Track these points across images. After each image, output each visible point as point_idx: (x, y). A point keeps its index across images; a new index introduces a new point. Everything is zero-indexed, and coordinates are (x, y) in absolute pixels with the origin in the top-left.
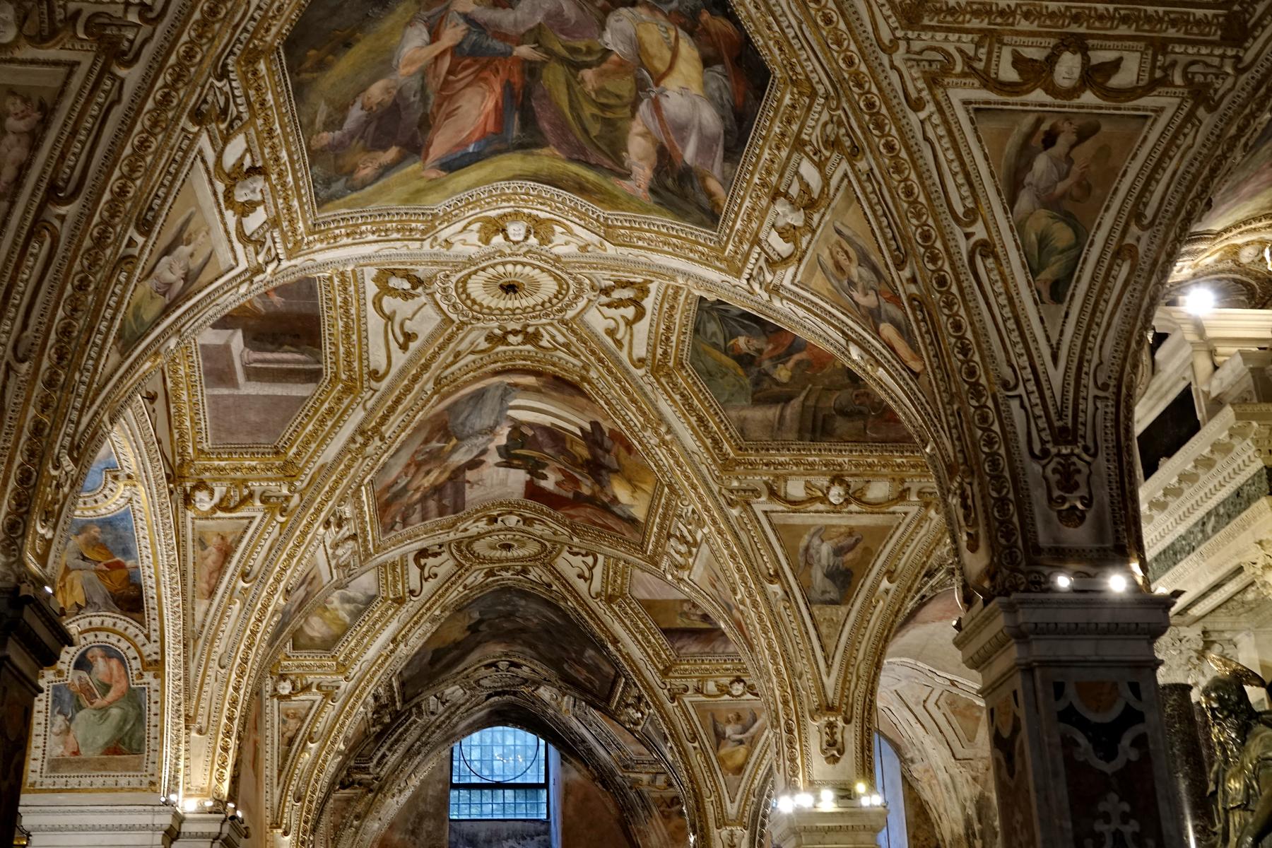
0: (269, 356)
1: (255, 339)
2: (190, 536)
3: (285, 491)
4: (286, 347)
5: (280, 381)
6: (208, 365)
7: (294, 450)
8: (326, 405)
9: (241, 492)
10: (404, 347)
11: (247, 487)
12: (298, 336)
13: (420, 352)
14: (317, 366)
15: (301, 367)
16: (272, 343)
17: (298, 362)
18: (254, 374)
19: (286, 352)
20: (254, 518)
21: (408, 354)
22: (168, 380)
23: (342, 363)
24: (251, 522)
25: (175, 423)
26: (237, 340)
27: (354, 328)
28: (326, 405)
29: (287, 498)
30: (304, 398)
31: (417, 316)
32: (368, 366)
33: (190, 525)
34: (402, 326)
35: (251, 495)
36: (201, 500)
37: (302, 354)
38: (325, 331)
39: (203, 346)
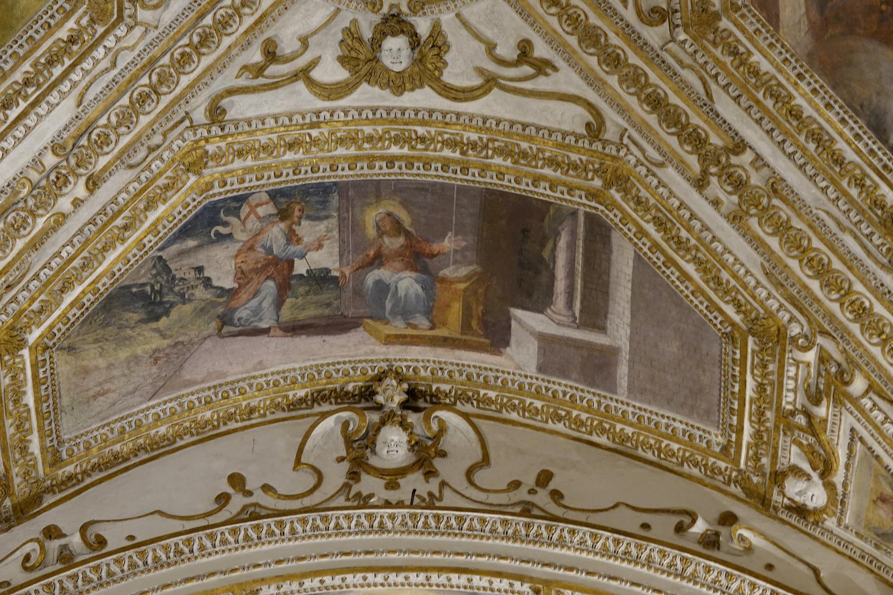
0: (560, 285)
1: (530, 295)
2: (869, 548)
3: (811, 356)
4: (546, 254)
5: (607, 284)
6: (574, 375)
7: (730, 310)
8: (650, 228)
9: (800, 429)
10: (543, 67)
11: (793, 413)
12: (524, 231)
13: (551, 39)
14: (581, 219)
15: (580, 243)
16: (538, 273)
17: (572, 247)
18: (594, 314)
19: (554, 258)
20: (852, 430)
21: (559, 62)
22: (594, 438)
23: (572, 178)
24: (861, 439)
25: (672, 462)
26: (527, 322)
27: (509, 140)
28: (650, 228)
29: (823, 359)
30: (638, 259)
31: (489, 33)
32: (578, 137)
33: (851, 537)
34: (502, 62)
35: (808, 415)
36: (800, 493)
37: (558, 234)
38: (508, 184)
39: (541, 369)
